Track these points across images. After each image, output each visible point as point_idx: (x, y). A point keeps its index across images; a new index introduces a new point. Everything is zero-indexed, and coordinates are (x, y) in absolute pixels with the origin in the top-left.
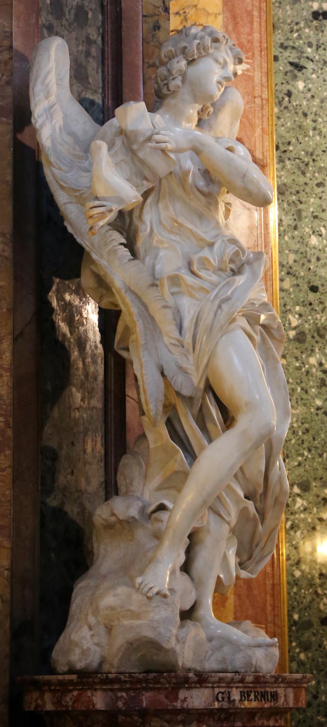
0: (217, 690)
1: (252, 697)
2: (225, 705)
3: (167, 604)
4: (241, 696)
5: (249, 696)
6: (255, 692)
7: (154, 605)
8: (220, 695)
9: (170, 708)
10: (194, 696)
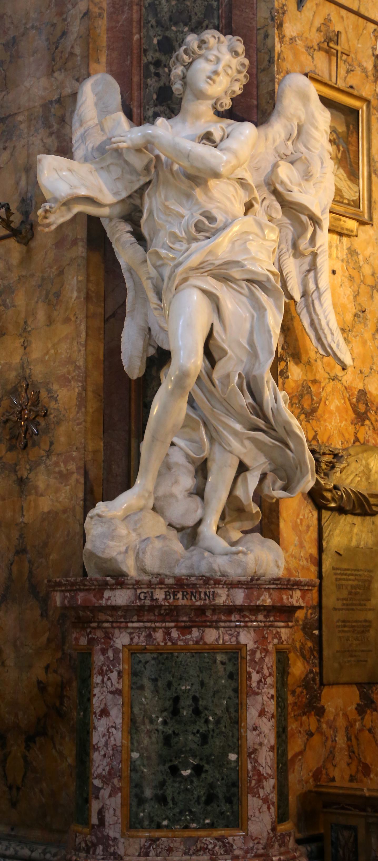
0: (139, 591)
1: (180, 595)
2: (148, 602)
3: (102, 522)
4: (166, 595)
5: (175, 595)
6: (183, 592)
7: (93, 523)
8: (142, 595)
9: (97, 605)
10: (117, 595)
